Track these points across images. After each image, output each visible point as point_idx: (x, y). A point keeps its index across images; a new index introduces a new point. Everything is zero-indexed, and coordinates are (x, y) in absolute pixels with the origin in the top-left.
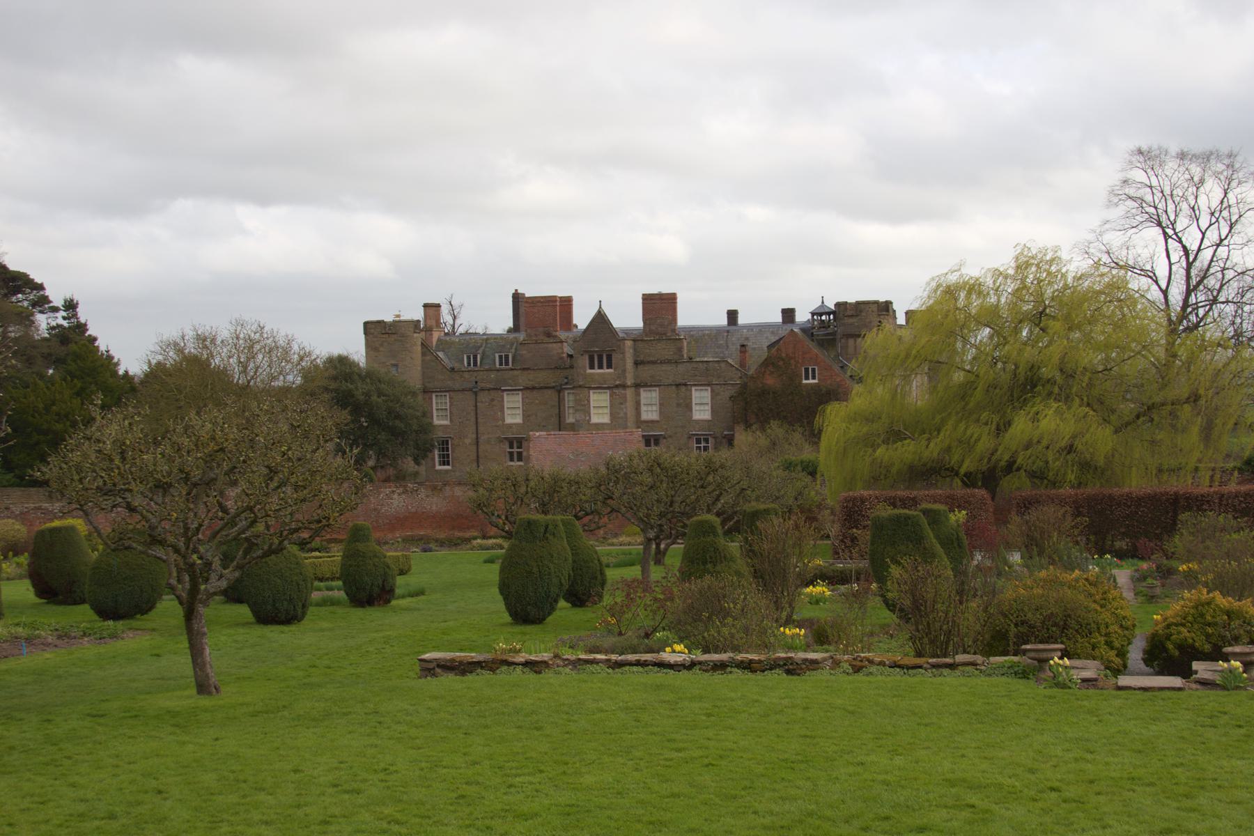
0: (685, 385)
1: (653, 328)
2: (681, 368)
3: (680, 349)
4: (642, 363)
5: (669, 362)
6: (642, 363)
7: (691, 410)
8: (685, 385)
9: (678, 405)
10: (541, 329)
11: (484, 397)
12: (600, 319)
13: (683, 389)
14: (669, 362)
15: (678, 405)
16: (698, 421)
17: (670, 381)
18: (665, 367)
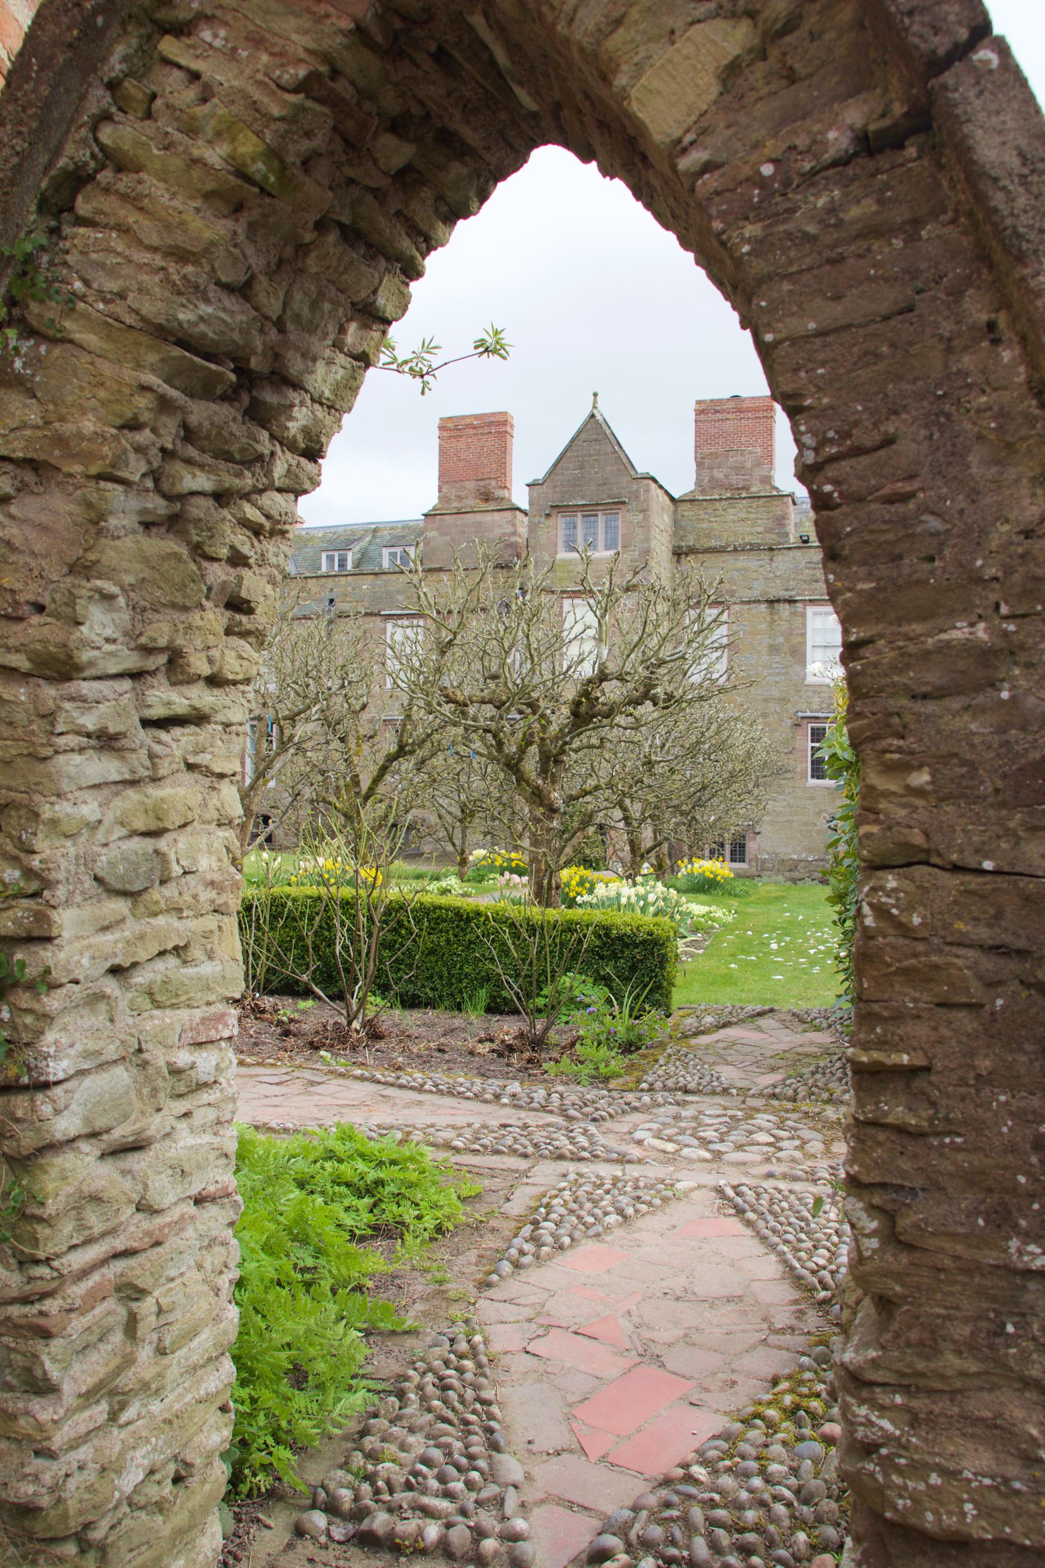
0: (791, 601)
1: (719, 475)
2: (783, 562)
3: (781, 521)
4: (692, 551)
5: (753, 548)
6: (692, 551)
7: (803, 662)
8: (791, 601)
9: (773, 649)
10: (471, 485)
11: (347, 632)
12: (594, 439)
13: (785, 609)
14: (753, 548)
15: (773, 649)
16: (817, 689)
17: (755, 594)
18: (744, 561)
